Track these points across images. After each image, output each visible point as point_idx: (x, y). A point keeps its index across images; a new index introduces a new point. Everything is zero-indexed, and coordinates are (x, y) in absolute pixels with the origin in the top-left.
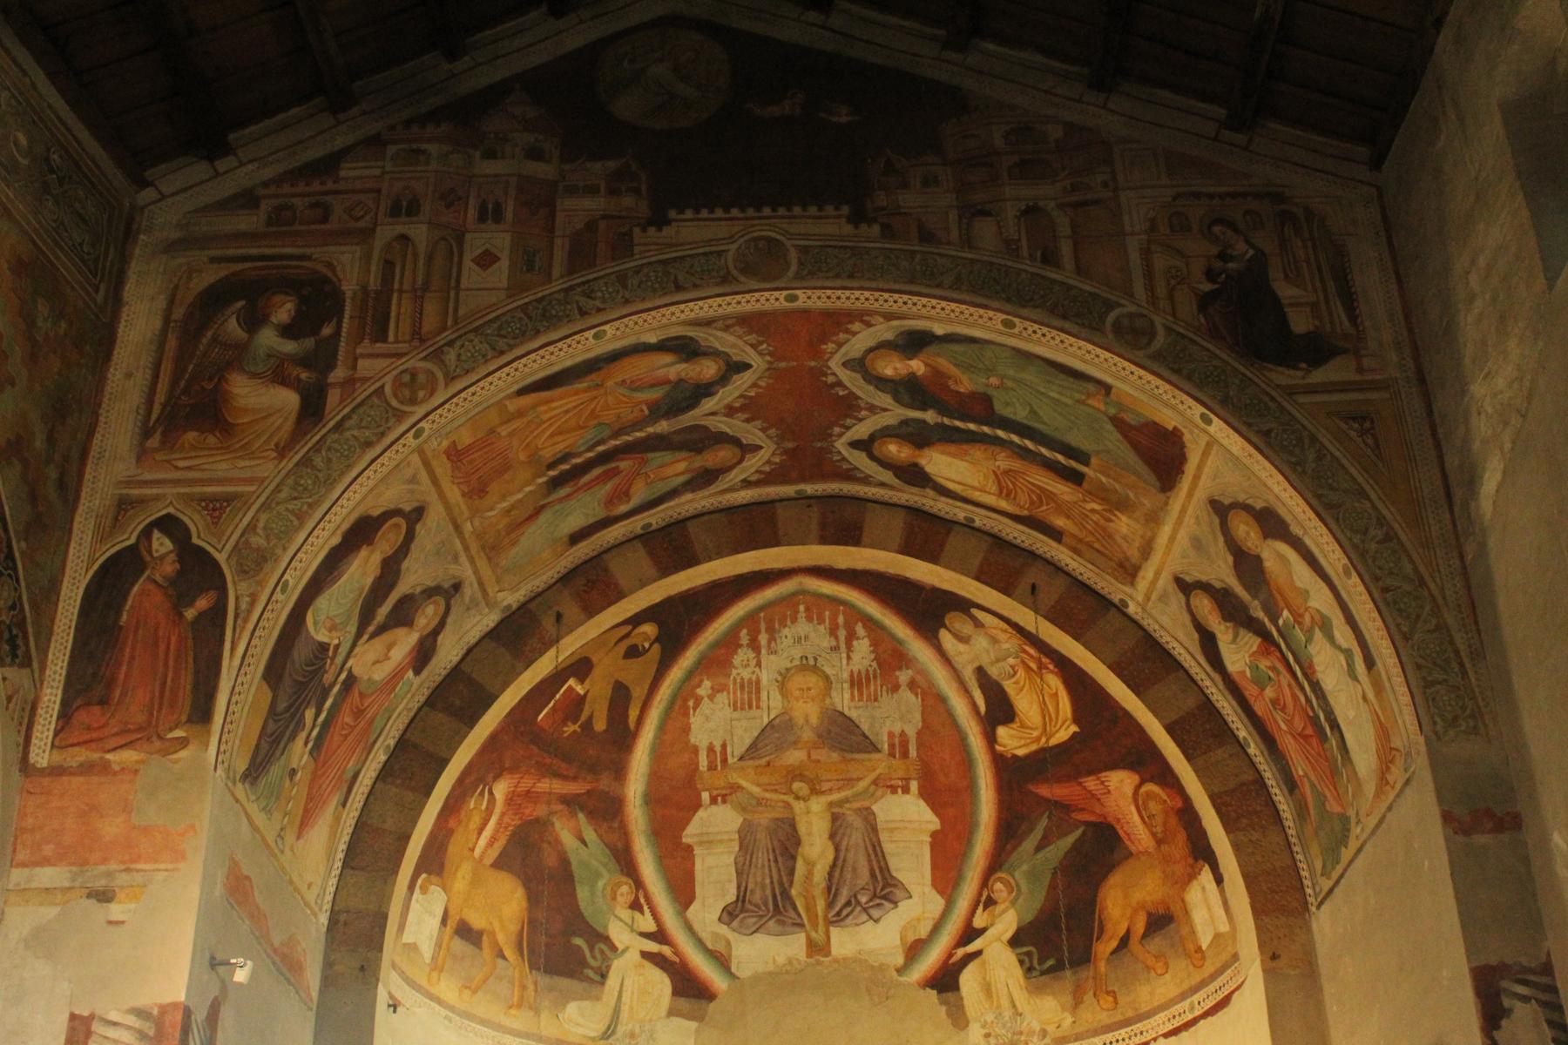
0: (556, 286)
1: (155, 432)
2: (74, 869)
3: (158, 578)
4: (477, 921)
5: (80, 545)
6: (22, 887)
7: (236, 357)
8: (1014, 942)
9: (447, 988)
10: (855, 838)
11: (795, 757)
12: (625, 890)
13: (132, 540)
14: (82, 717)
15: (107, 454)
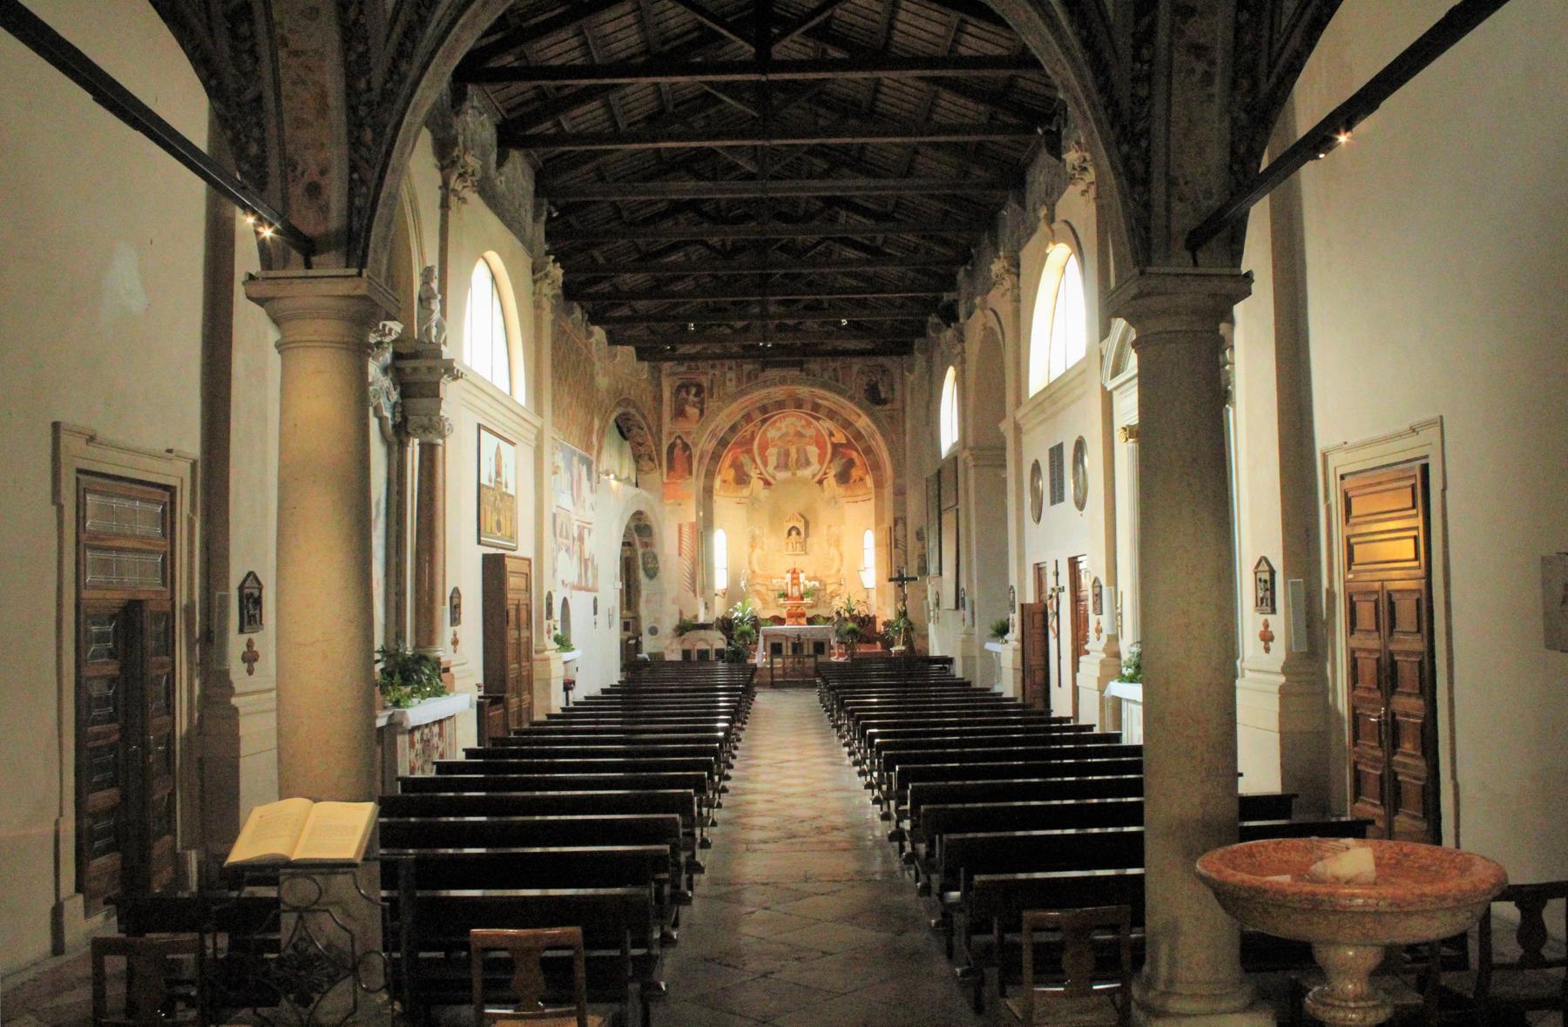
8: (835, 476)
9: (722, 493)
11: (789, 438)
12: (754, 466)
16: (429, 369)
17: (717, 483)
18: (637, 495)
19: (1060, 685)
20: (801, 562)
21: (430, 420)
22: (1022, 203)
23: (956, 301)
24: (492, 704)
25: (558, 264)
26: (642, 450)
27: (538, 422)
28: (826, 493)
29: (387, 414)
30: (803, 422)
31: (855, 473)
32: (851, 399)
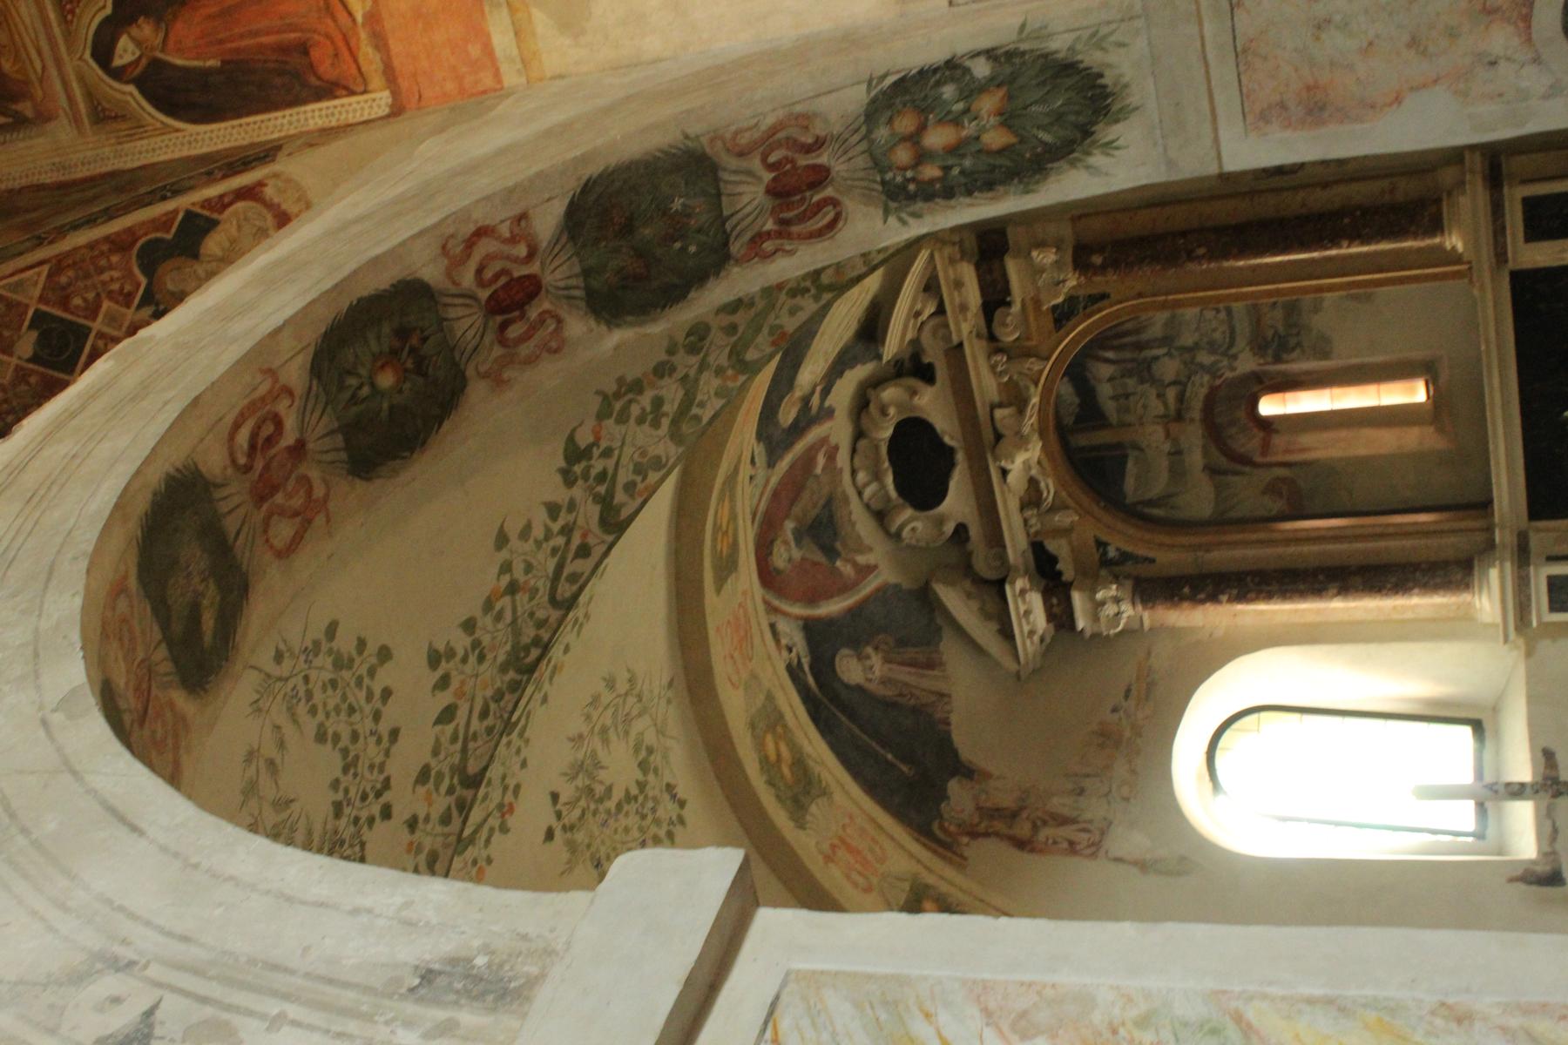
1: (17, 112)
2: (487, 9)
3: (161, 35)
5: (154, 150)
6: (519, 66)
13: (131, 88)
14: (326, 69)
15: (57, 160)
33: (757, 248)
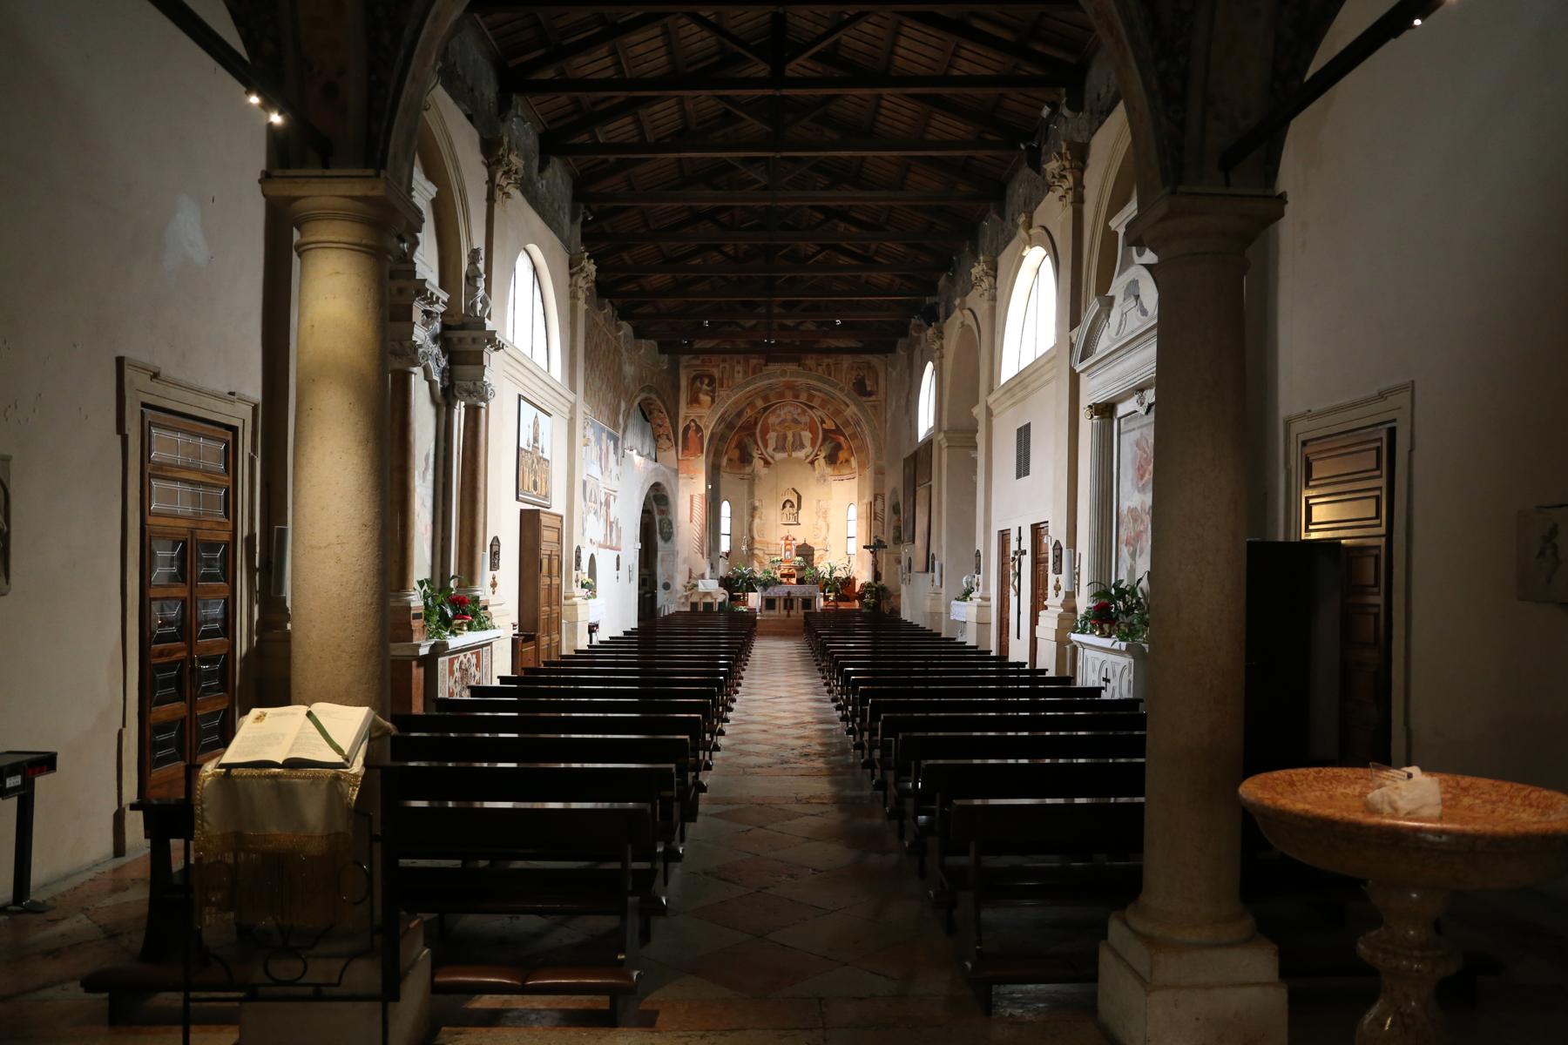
0: (749, 378)
4: (732, 457)
7: (699, 390)
8: (825, 458)
9: (728, 470)
10: (797, 438)
11: (786, 424)
16: (474, 340)
17: (724, 461)
18: (656, 469)
19: (1018, 638)
20: (793, 531)
21: (475, 384)
22: (1002, 214)
23: (937, 304)
24: (524, 641)
25: (592, 261)
26: (661, 430)
27: (571, 397)
28: (817, 472)
29: (437, 378)
30: (799, 410)
31: (842, 455)
32: (842, 390)
33: (658, 508)
